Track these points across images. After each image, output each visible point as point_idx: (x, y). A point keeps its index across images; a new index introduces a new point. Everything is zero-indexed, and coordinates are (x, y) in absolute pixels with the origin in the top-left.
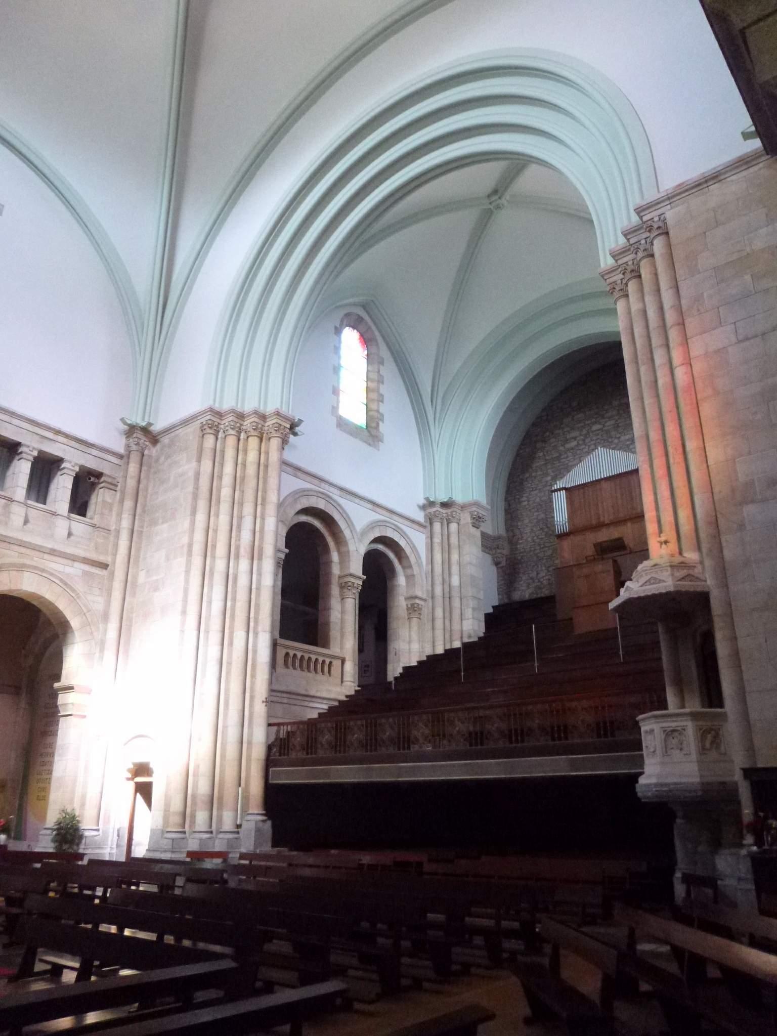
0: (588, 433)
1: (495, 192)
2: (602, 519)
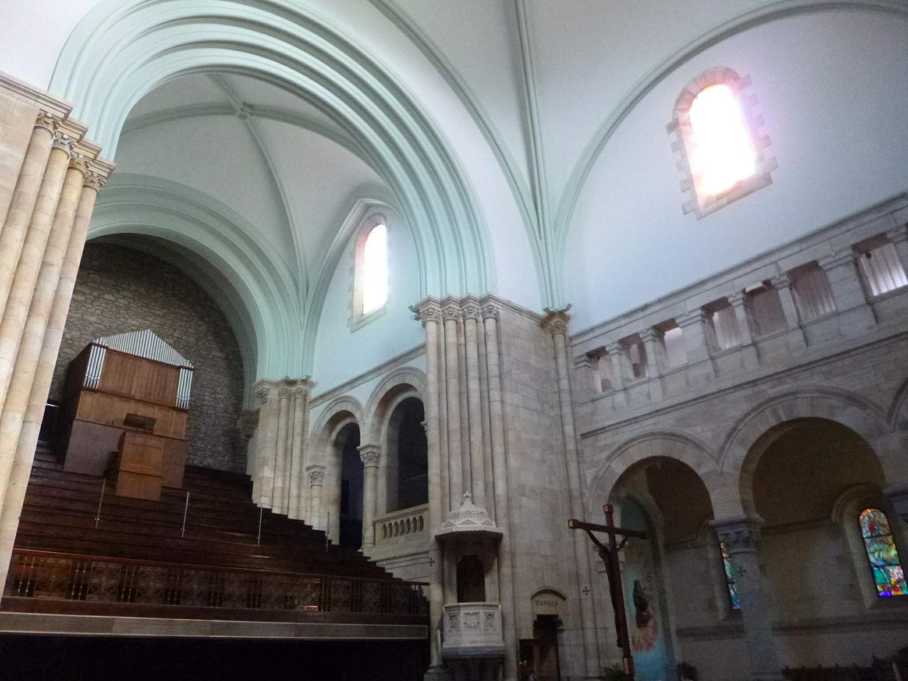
0: (99, 297)
1: (251, 107)
2: (133, 393)
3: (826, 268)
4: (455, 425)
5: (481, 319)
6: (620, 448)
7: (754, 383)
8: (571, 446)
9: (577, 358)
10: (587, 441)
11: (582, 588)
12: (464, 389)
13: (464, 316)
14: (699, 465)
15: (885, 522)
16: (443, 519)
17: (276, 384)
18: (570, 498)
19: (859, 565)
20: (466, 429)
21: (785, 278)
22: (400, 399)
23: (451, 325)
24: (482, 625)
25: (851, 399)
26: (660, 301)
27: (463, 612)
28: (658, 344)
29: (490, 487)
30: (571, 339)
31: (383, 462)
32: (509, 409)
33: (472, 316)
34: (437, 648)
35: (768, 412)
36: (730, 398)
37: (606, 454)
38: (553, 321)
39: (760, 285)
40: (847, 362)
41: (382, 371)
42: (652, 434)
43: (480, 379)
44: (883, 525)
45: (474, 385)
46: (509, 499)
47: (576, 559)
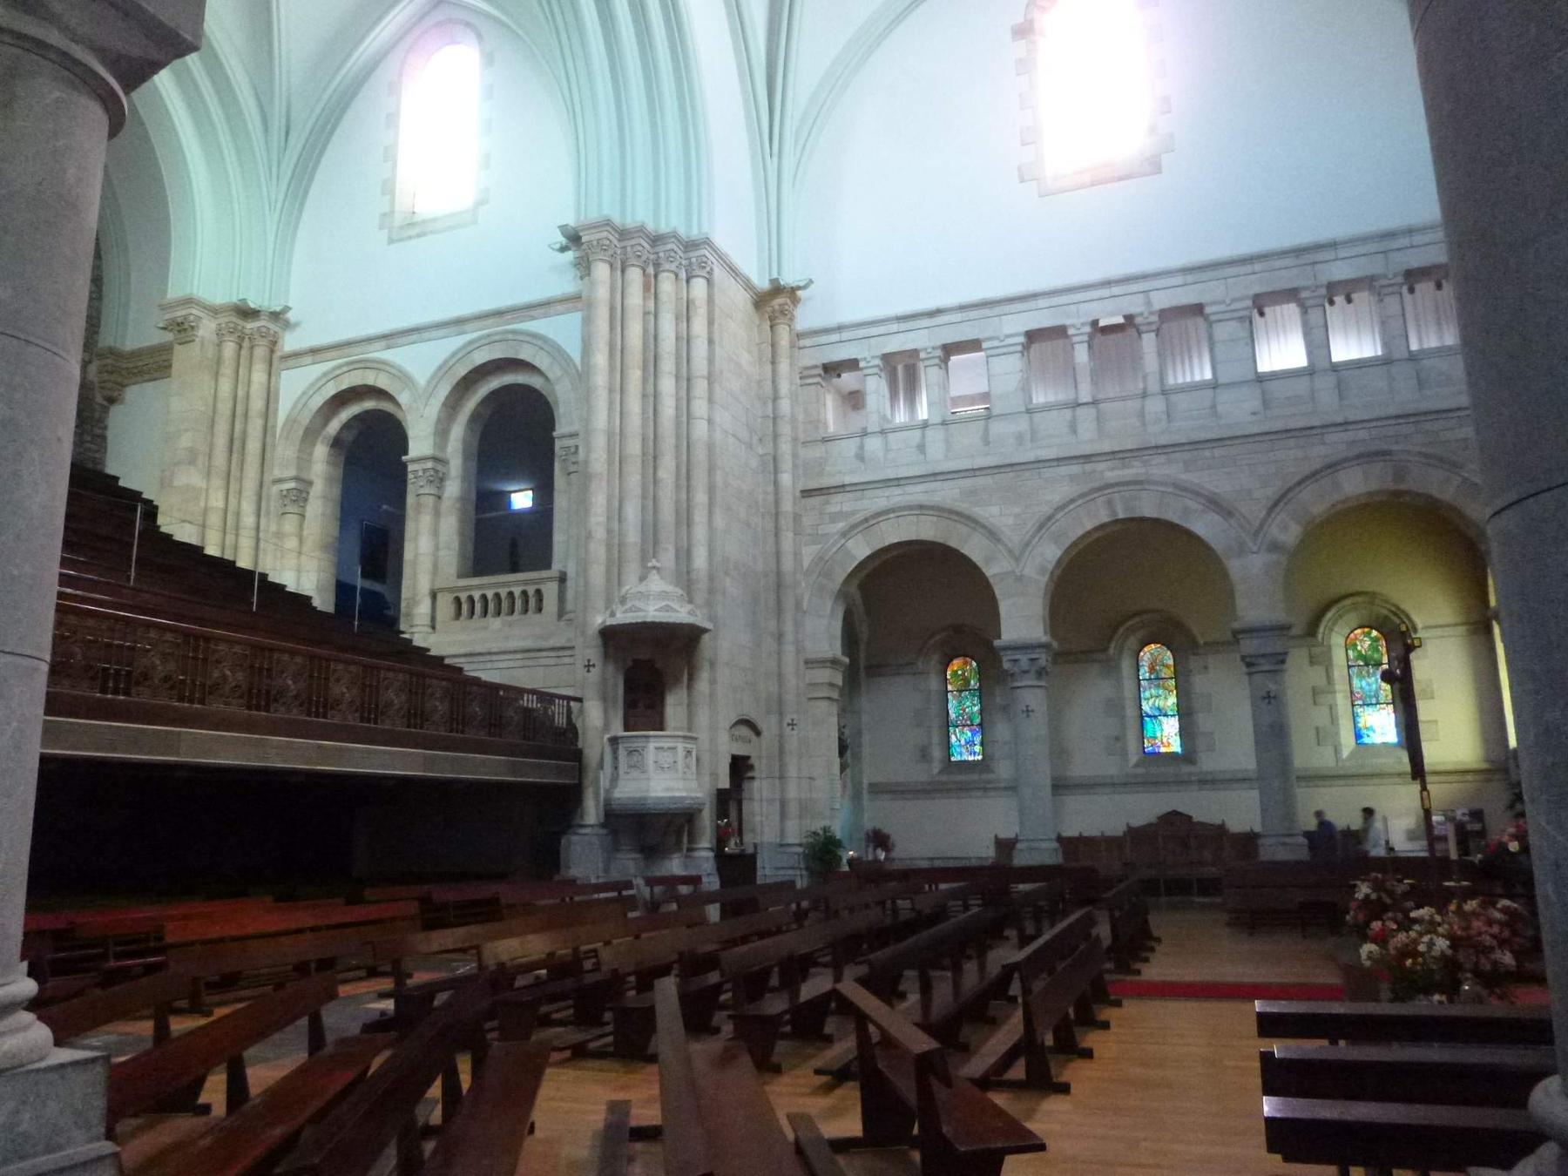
3: (1213, 318)
4: (634, 447)
5: (683, 275)
6: (866, 520)
7: (1087, 458)
8: (787, 506)
9: (807, 368)
10: (815, 501)
11: (788, 720)
12: (650, 389)
13: (657, 265)
14: (988, 560)
15: (1171, 662)
16: (609, 602)
17: (214, 311)
18: (779, 586)
19: (1131, 712)
20: (652, 458)
21: (1154, 318)
22: (495, 383)
23: (635, 275)
24: (680, 765)
25: (1214, 503)
26: (962, 308)
27: (652, 745)
28: (943, 372)
29: (685, 554)
30: (800, 336)
31: (453, 488)
32: (718, 436)
33: (673, 267)
34: (597, 794)
35: (1100, 501)
36: (1048, 473)
37: (841, 525)
38: (774, 301)
39: (1121, 320)
40: (1217, 452)
41: (468, 327)
42: (921, 507)
43: (678, 378)
44: (1167, 666)
45: (667, 385)
46: (711, 578)
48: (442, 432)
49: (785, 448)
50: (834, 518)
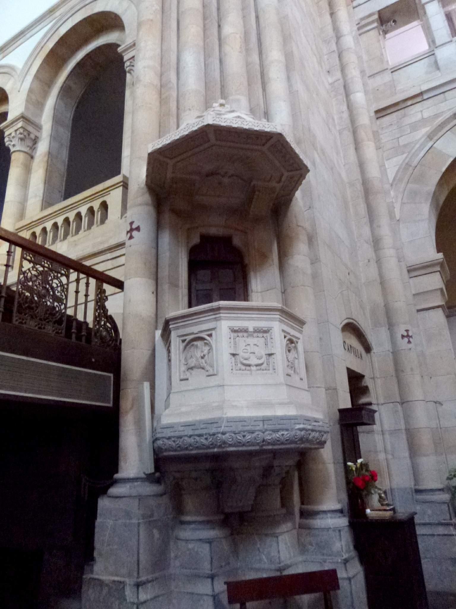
9: (362, 19)
11: (401, 330)
18: (367, 190)
31: (43, 147)
34: (139, 422)
37: (425, 130)
47: (383, 282)
48: (36, 100)
49: (353, 72)
50: (415, 127)
